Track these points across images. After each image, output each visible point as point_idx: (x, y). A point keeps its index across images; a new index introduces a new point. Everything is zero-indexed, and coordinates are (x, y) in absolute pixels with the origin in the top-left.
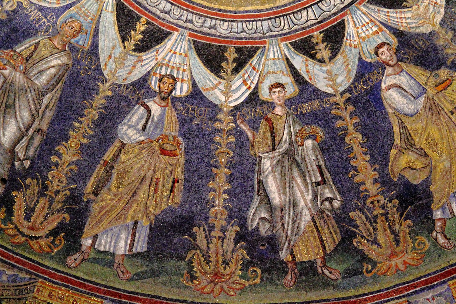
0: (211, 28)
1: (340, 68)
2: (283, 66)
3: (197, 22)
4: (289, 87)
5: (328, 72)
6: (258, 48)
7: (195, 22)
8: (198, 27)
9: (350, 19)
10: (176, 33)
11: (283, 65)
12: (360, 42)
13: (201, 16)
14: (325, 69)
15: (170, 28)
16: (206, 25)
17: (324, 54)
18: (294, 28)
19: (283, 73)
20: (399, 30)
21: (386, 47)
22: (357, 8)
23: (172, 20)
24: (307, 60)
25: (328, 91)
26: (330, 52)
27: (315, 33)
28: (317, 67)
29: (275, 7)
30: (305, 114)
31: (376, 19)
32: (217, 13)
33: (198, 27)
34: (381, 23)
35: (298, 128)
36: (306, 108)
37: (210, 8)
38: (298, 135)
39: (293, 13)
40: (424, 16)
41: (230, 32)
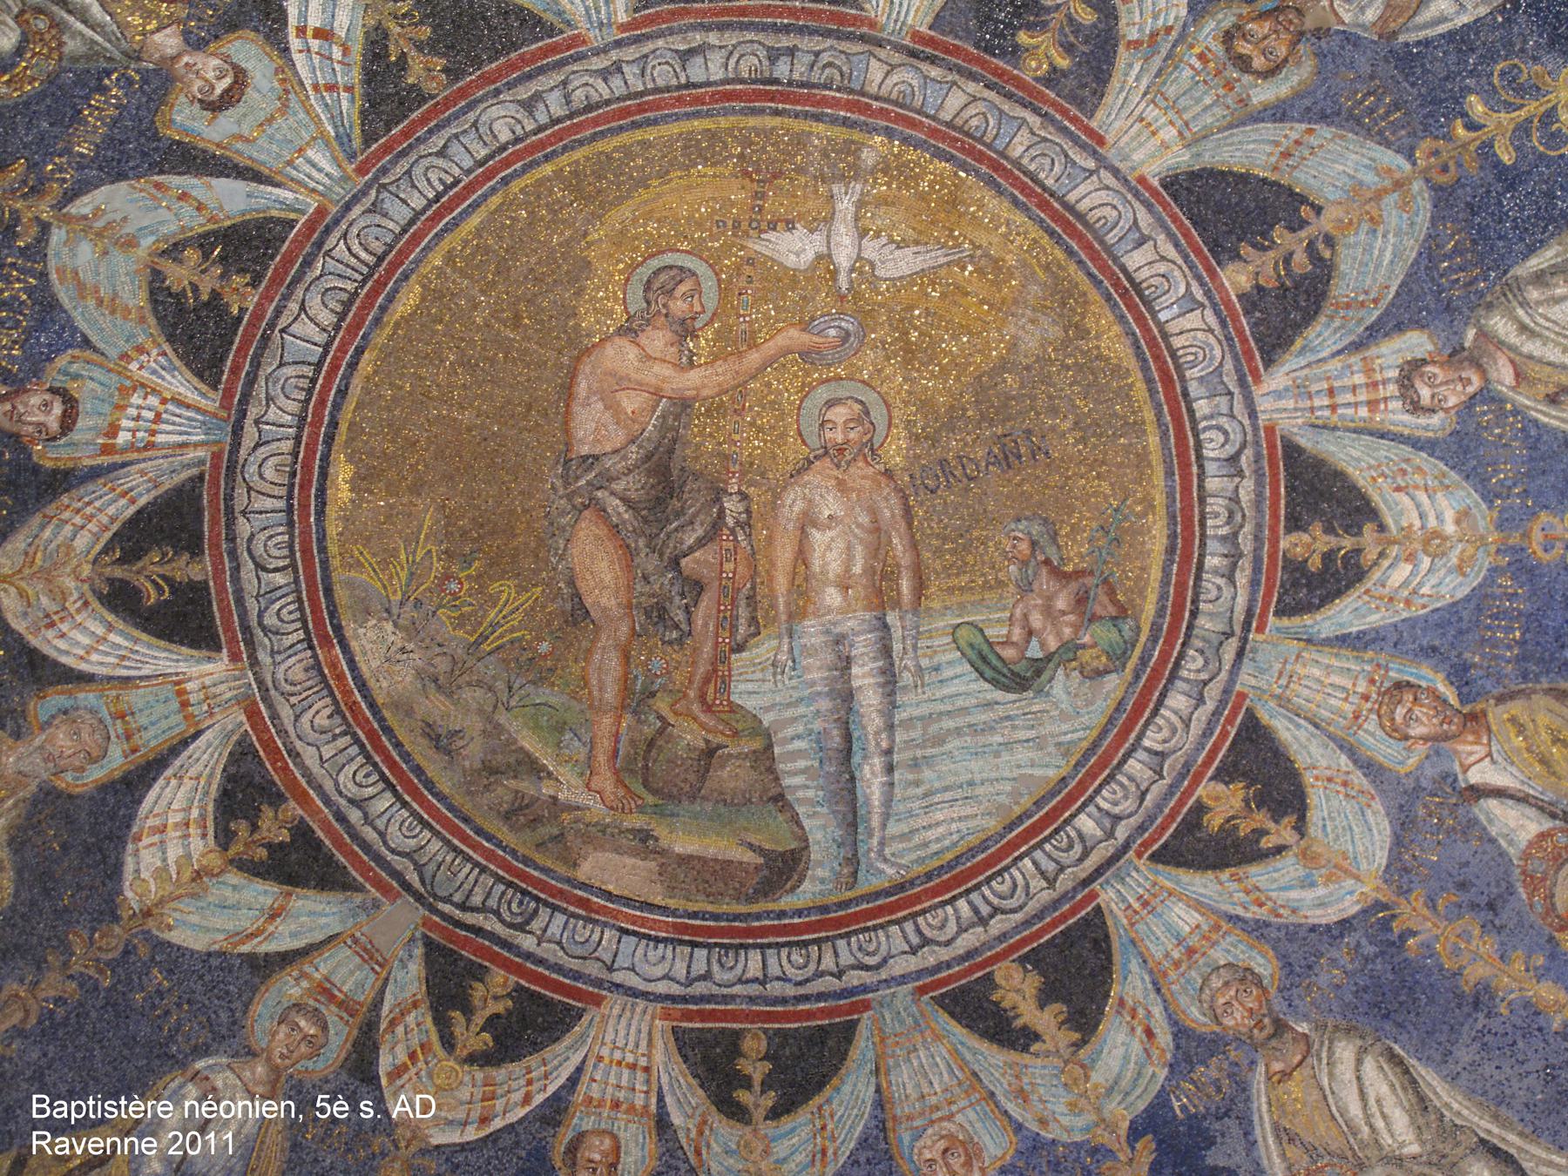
1: (111, 277)
2: (263, 154)
3: (588, 86)
4: (194, 119)
5: (130, 243)
6: (368, 139)
10: (622, 17)
11: (263, 157)
12: (128, 378)
14: (147, 242)
15: (650, 20)
16: (557, 94)
19: (247, 141)
20: (67, 490)
21: (54, 426)
23: (660, 43)
25: (86, 199)
26: (175, 289)
28: (173, 228)
29: (412, 271)
30: (87, 98)
31: (144, 460)
34: (124, 465)
35: (72, 46)
36: (99, 113)
37: (581, 143)
38: (54, 32)
40: (47, 575)
41: (475, 125)
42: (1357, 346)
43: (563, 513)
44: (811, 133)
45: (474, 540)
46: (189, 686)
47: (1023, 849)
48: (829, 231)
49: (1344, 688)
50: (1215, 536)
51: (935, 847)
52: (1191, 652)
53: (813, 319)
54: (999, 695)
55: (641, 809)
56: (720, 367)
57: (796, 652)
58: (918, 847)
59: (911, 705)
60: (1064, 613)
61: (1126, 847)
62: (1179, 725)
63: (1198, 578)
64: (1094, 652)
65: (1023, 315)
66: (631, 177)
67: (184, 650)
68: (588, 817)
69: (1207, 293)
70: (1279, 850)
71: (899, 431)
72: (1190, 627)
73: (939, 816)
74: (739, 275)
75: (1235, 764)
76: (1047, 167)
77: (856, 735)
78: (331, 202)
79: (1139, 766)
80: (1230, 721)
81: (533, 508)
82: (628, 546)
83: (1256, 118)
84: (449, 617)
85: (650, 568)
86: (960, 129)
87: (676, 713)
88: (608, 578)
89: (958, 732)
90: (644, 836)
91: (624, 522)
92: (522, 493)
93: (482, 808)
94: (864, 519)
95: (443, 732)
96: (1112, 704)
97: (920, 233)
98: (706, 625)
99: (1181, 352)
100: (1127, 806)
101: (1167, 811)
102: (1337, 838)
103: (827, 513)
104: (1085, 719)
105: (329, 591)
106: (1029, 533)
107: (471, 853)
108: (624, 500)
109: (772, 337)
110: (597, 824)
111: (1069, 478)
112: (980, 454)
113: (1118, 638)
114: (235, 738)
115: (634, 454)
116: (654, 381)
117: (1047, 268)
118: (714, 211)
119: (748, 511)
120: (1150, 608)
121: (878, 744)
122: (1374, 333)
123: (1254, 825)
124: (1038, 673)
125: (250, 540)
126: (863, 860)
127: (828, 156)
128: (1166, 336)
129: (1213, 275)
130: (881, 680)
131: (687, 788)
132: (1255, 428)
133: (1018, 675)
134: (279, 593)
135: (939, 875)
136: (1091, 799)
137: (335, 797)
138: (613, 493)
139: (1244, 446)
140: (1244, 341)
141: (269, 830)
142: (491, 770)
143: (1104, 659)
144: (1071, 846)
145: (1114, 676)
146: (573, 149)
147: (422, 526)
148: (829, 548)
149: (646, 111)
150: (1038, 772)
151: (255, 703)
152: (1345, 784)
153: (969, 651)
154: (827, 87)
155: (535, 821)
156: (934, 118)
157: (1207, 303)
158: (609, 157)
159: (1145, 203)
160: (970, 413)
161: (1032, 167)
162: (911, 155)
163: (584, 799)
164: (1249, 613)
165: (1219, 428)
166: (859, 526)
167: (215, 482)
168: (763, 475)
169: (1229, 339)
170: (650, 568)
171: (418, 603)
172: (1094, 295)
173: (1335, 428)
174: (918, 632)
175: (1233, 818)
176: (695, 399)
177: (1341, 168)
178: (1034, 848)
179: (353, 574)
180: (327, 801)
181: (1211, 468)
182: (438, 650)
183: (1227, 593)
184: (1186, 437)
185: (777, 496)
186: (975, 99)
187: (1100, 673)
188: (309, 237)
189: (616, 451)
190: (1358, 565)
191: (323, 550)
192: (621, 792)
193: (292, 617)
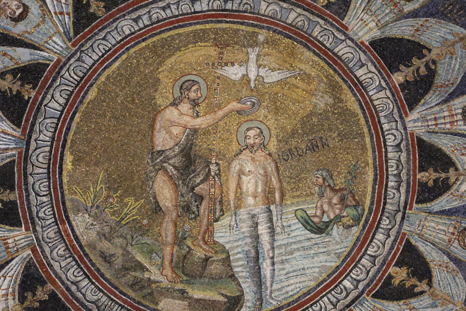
0: (139, 17)
2: (36, 39)
4: (8, 24)
6: (76, 34)
7: (159, 11)
8: (152, 8)
9: (14, 133)
11: (36, 40)
13: (158, 21)
16: (146, 16)
17: (6, 83)
18: (59, 81)
19: (29, 33)
22: (19, 148)
24: (16, 63)
27: (34, 94)
29: (94, 83)
32: (145, 35)
33: (152, 8)
37: (155, 35)
39: (73, 92)
41: (116, 28)
42: (446, 101)
43: (151, 172)
44: (240, 29)
45: (118, 183)
46: (9, 241)
47: (324, 293)
48: (247, 66)
49: (445, 231)
50: (392, 174)
51: (291, 293)
52: (384, 218)
53: (241, 98)
54: (313, 235)
55: (182, 282)
56: (208, 117)
57: (238, 221)
58: (284, 294)
59: (281, 240)
60: (336, 204)
61: (363, 292)
62: (381, 245)
63: (386, 190)
64: (348, 218)
65: (318, 95)
66: (174, 47)
67: (7, 227)
68: (162, 285)
69: (387, 84)
70: (422, 293)
71: (274, 139)
72: (384, 208)
73: (292, 281)
74: (214, 83)
75: (403, 260)
76: (327, 40)
77: (260, 251)
78: (63, 57)
79: (366, 261)
80: (400, 243)
81: (140, 170)
82: (175, 184)
83: (407, 16)
84: (109, 212)
85: (184, 191)
86: (294, 26)
87: (194, 245)
88: (168, 195)
89: (298, 249)
90: (183, 292)
91: (174, 175)
92: (136, 165)
93: (122, 283)
94: (262, 172)
95: (108, 255)
96: (355, 238)
97: (280, 65)
98: (204, 212)
99: (377, 107)
100: (362, 276)
101: (377, 278)
102: (445, 288)
103: (248, 170)
104: (345, 244)
105: (64, 203)
106: (322, 175)
107: (118, 301)
108: (175, 167)
109: (227, 105)
110: (165, 288)
111: (336, 154)
112: (303, 147)
113: (356, 213)
114: (27, 260)
115: (177, 149)
116: (184, 123)
117: (327, 77)
118: (205, 59)
119: (219, 170)
120: (368, 202)
121: (268, 255)
122: (452, 96)
123: (411, 283)
124: (327, 227)
125: (33, 185)
126: (264, 299)
127: (246, 38)
128: (372, 101)
129: (389, 77)
130: (269, 231)
131: (198, 273)
132: (406, 134)
133: (320, 228)
134: (44, 204)
135: (293, 304)
136: (348, 274)
137: (66, 282)
138: (169, 164)
139: (402, 140)
140: (401, 101)
141: (40, 296)
142: (126, 269)
143: (351, 221)
144: (342, 292)
145: (355, 227)
146: (153, 37)
147: (99, 178)
148: (249, 182)
149: (179, 22)
150: (328, 264)
151: (35, 246)
152: (446, 267)
153: (301, 220)
154: (245, 12)
155: (143, 287)
156: (285, 22)
157: (387, 88)
158: (166, 40)
159: (364, 52)
160: (300, 131)
161: (321, 40)
162: (278, 37)
163: (161, 278)
164: (406, 203)
165: (392, 134)
166: (260, 174)
167: (19, 163)
168: (224, 156)
169: (395, 100)
170: (184, 191)
171: (98, 207)
172: (344, 86)
173: (437, 133)
174: (282, 213)
175: (403, 280)
176: (199, 129)
177: (439, 34)
178: (328, 293)
179: (73, 196)
180: (63, 283)
181: (390, 149)
182: (105, 224)
183: (397, 195)
184: (380, 138)
185: (230, 164)
186: (300, 15)
187: (349, 227)
188: (54, 70)
189: (170, 149)
190: (448, 184)
191: (61, 188)
192: (174, 275)
193: (50, 213)
